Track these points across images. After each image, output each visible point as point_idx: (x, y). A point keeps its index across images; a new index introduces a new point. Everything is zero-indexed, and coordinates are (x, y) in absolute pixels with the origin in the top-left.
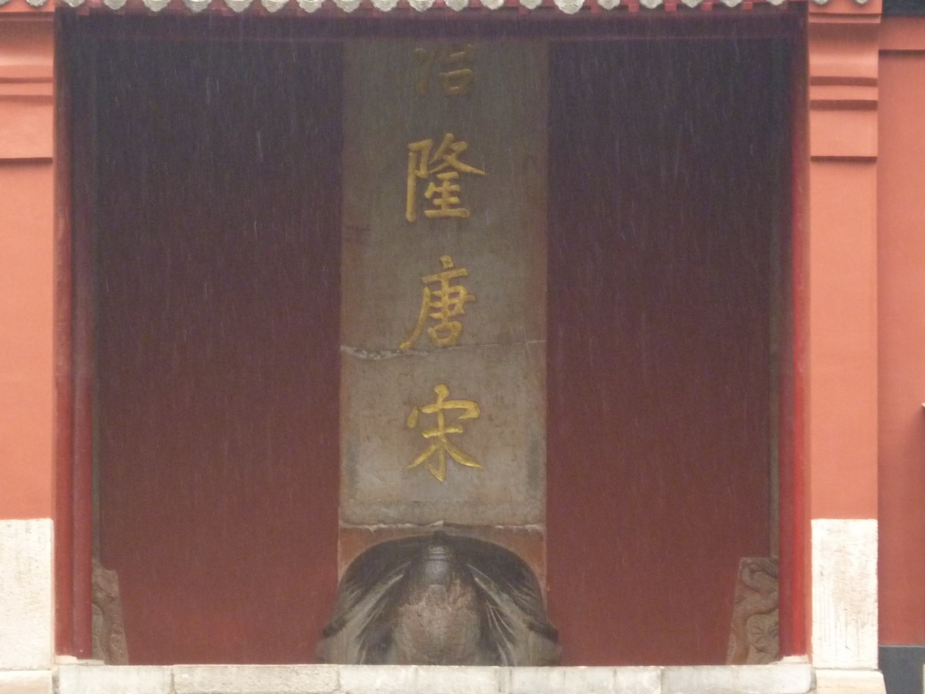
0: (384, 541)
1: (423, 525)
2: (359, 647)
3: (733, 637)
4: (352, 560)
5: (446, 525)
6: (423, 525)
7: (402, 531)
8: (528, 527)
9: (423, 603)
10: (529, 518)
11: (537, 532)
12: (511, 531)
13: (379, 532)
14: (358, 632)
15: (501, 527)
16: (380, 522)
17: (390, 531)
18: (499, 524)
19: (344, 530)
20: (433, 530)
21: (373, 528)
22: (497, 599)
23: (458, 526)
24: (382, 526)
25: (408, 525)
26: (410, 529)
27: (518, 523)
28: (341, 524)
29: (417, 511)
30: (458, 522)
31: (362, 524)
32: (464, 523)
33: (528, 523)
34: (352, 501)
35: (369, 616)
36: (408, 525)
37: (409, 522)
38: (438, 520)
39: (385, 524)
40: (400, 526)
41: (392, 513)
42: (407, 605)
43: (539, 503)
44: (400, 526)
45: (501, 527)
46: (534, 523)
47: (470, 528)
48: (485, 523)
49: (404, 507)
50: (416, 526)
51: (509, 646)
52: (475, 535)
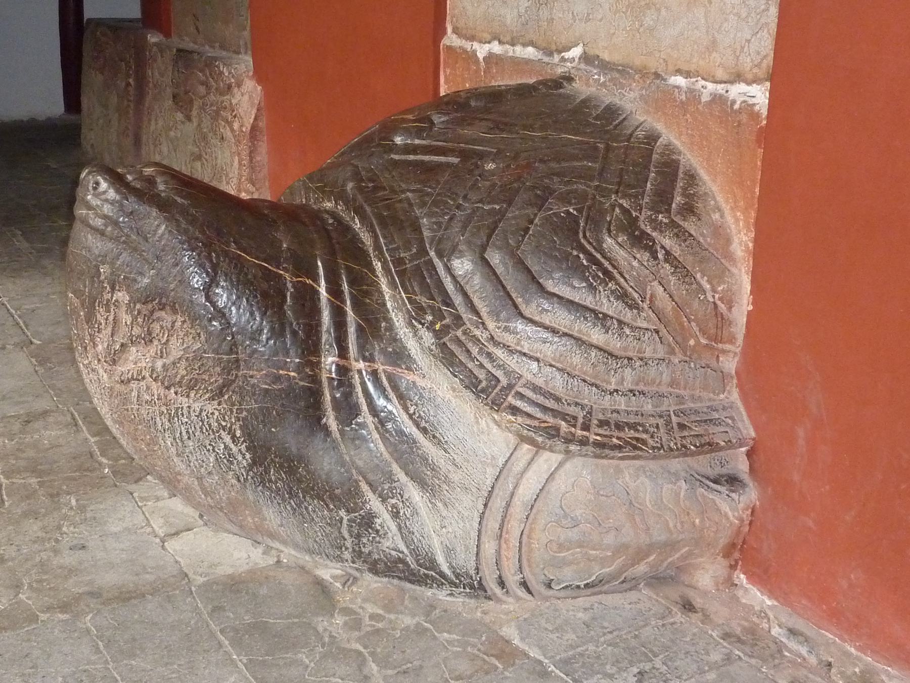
5: (586, 58)
10: (747, 63)
12: (693, 95)
18: (679, 72)
19: (449, 48)
22: (411, 345)
23: (605, 66)
25: (530, 52)
26: (527, 61)
27: (720, 74)
30: (606, 56)
33: (738, 77)
36: (530, 52)
37: (532, 43)
38: (576, 45)
39: (500, 42)
46: (754, 82)
48: (653, 65)
51: (414, 493)
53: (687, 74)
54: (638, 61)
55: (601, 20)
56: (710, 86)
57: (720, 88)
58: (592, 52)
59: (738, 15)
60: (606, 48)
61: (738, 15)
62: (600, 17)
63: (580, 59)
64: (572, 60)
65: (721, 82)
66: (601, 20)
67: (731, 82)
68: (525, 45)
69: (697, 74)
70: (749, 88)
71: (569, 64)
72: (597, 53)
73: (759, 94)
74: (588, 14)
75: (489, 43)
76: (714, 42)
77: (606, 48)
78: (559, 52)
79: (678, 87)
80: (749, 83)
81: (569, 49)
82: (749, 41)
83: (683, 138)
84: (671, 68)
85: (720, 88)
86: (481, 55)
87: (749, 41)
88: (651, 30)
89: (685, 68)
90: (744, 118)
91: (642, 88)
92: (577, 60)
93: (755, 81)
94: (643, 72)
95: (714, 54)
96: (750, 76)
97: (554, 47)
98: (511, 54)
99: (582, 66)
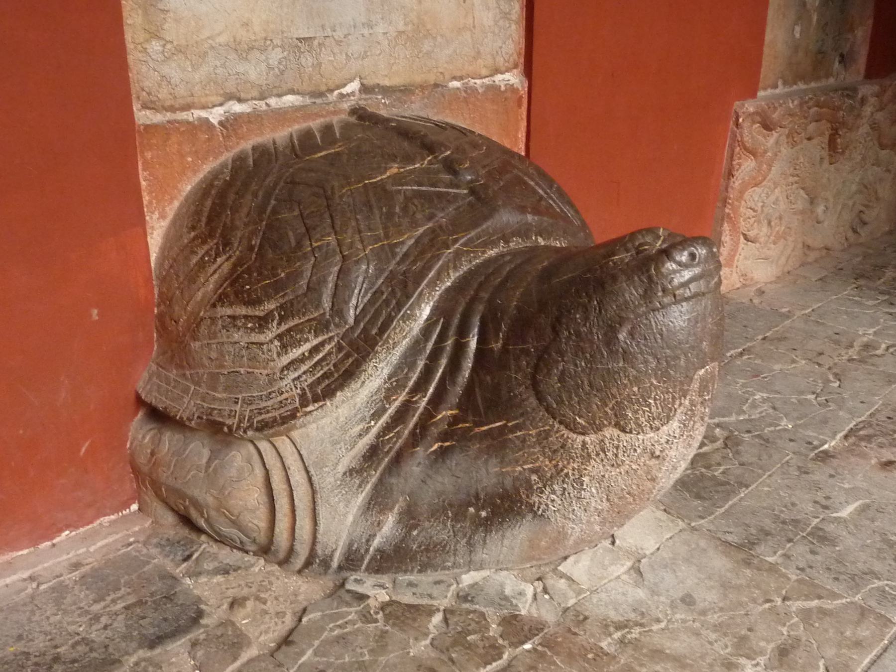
0: (247, 145)
1: (321, 95)
2: (361, 499)
3: (726, 226)
4: (176, 204)
5: (365, 89)
6: (321, 95)
7: (282, 116)
8: (498, 78)
9: (675, 424)
10: (500, 61)
11: (512, 89)
12: (474, 90)
13: (231, 124)
14: (348, 458)
15: (456, 84)
16: (230, 97)
17: (254, 119)
18: (454, 78)
20: (346, 106)
21: (215, 115)
23: (386, 91)
24: (237, 108)
25: (290, 100)
26: (296, 109)
27: (484, 72)
28: (143, 117)
29: (307, 60)
30: (387, 82)
31: (187, 107)
32: (396, 81)
33: (497, 71)
34: (155, 46)
35: (376, 416)
36: (290, 100)
37: (292, 92)
38: (351, 80)
39: (240, 100)
40: (273, 102)
41: (254, 71)
42: (610, 432)
43: (514, 27)
44: (273, 102)
45: (456, 84)
46: (507, 71)
47: (406, 90)
48: (432, 79)
49: (276, 56)
50: (308, 101)
52: (414, 109)
53: (461, 78)
54: (418, 79)
55: (380, 54)
56: (478, 81)
57: (486, 81)
58: (369, 82)
59: (493, 33)
60: (386, 76)
61: (493, 33)
62: (378, 52)
63: (360, 91)
64: (353, 94)
65: (485, 77)
66: (380, 54)
67: (491, 75)
68: (279, 96)
69: (468, 76)
70: (503, 76)
71: (352, 98)
72: (377, 81)
73: (511, 78)
74: (365, 52)
75: (221, 105)
76: (479, 53)
77: (386, 76)
78: (332, 91)
79: (458, 89)
80: (502, 73)
81: (345, 85)
82: (501, 48)
83: (468, 122)
84: (447, 77)
85: (486, 81)
86: (215, 121)
87: (501, 48)
88: (428, 53)
89: (459, 74)
90: (509, 94)
91: (423, 98)
92: (357, 92)
93: (508, 70)
94: (422, 87)
95: (480, 60)
96: (503, 69)
97: (323, 88)
98: (264, 107)
99: (364, 96)
